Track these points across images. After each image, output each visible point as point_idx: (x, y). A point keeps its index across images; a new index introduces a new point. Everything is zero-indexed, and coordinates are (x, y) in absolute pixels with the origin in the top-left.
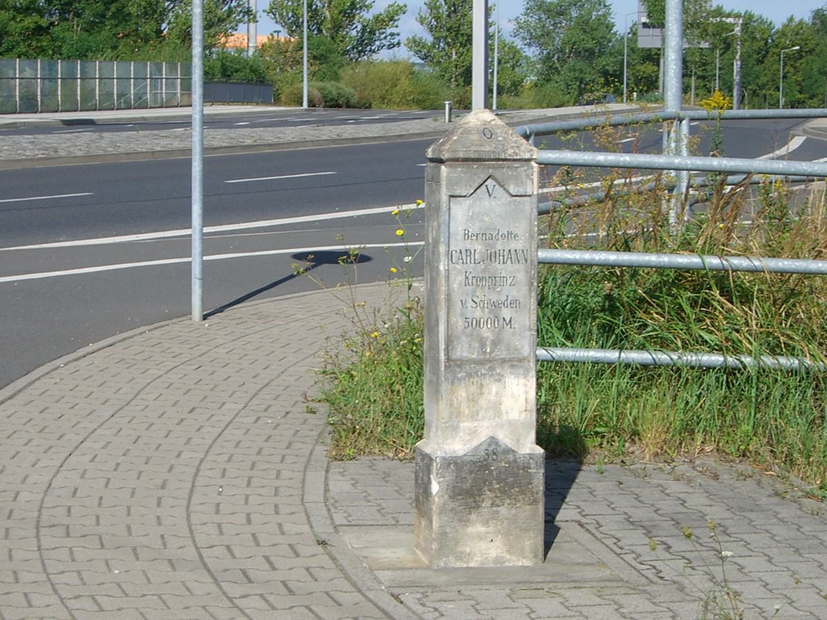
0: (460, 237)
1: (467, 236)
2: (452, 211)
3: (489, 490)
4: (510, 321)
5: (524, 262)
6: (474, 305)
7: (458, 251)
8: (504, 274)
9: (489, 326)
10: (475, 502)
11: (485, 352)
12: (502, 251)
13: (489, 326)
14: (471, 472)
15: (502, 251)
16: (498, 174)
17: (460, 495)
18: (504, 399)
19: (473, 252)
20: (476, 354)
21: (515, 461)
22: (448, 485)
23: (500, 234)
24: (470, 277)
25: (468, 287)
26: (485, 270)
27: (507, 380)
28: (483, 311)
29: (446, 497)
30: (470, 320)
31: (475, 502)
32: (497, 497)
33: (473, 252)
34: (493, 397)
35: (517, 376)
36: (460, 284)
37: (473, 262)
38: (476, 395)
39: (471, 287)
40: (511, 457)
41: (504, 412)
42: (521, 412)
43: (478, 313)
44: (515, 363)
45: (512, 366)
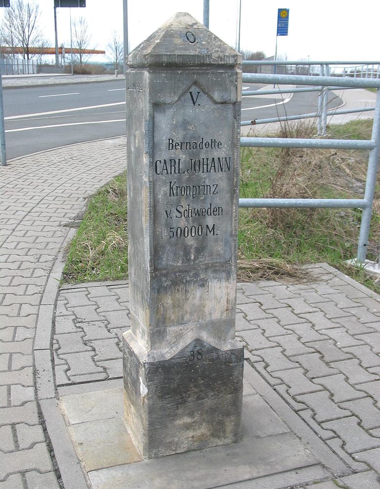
0: (164, 147)
1: (172, 145)
2: (156, 120)
3: (195, 387)
4: (213, 228)
5: (227, 170)
6: (179, 215)
7: (163, 161)
8: (207, 183)
9: (193, 235)
10: (182, 398)
11: (189, 260)
12: (205, 160)
13: (193, 235)
14: (178, 373)
15: (205, 160)
16: (203, 80)
17: (168, 394)
18: (207, 302)
19: (177, 161)
20: (181, 262)
21: (218, 358)
22: (156, 387)
23: (204, 143)
24: (174, 187)
25: (172, 197)
26: (189, 180)
27: (210, 283)
28: (187, 221)
29: (155, 398)
30: (174, 230)
31: (182, 398)
32: (201, 391)
33: (177, 161)
34: (197, 302)
35: (220, 280)
36: (165, 194)
37: (177, 171)
38: (181, 301)
39: (176, 197)
40: (214, 355)
41: (207, 313)
42: (222, 313)
43: (183, 223)
44: (218, 268)
45: (215, 271)
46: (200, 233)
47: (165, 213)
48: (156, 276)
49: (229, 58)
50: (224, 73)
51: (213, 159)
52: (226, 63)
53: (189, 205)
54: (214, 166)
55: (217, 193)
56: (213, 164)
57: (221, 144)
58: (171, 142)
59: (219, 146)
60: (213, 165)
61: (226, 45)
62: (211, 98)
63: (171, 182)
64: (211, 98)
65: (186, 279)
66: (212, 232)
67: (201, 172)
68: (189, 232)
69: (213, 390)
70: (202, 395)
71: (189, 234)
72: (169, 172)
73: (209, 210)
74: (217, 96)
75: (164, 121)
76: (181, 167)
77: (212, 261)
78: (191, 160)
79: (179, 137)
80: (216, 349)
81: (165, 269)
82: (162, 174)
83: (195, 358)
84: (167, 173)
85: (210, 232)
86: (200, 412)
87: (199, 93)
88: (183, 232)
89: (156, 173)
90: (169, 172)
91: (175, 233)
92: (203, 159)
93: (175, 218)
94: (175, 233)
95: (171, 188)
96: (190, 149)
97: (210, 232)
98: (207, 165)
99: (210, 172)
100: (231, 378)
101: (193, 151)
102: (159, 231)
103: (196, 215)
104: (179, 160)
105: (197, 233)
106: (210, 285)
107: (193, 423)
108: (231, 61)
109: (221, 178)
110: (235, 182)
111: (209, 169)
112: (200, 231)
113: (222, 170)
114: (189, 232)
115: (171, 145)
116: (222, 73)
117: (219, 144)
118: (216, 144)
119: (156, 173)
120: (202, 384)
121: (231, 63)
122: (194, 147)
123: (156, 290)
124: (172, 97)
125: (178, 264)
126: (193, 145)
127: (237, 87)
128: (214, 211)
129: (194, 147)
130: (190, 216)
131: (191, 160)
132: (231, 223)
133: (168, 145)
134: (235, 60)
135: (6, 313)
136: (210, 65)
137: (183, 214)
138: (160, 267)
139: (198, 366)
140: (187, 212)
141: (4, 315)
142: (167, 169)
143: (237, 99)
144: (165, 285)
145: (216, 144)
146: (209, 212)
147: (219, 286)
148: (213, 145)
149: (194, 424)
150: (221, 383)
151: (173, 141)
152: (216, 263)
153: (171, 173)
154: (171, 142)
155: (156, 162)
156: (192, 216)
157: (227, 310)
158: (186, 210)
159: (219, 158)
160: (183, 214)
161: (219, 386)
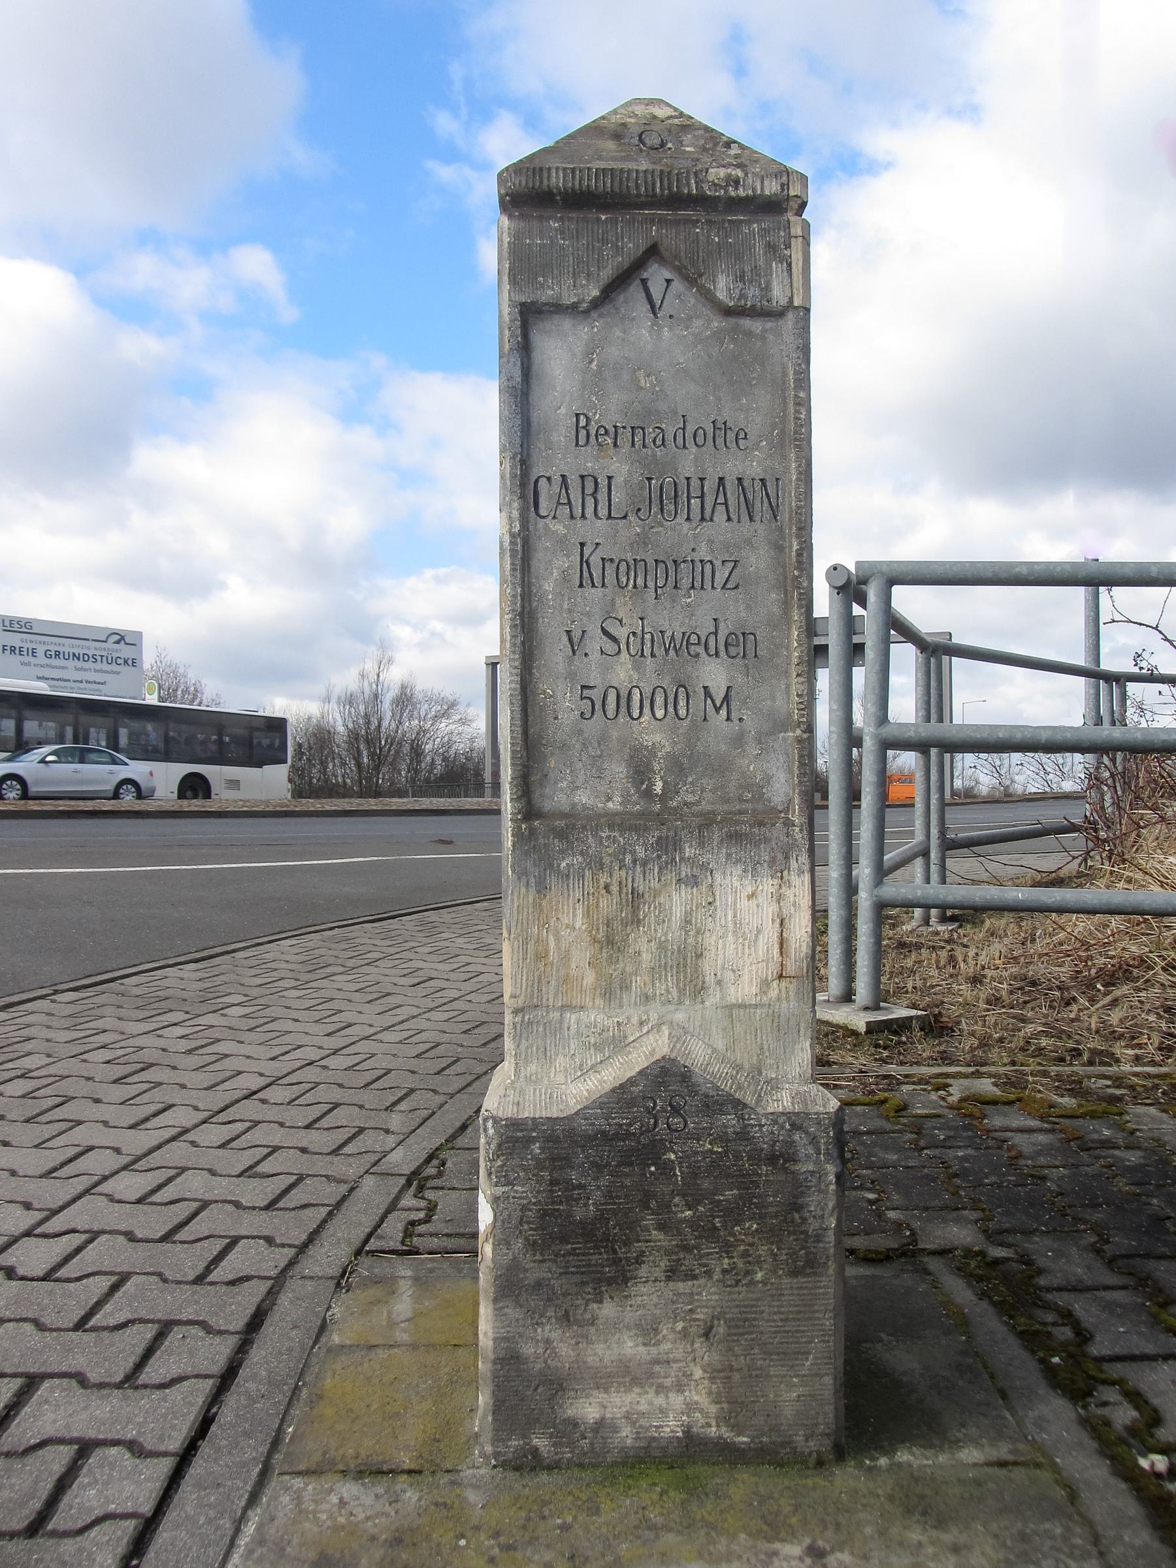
0: (561, 435)
1: (585, 432)
2: (536, 356)
3: (661, 1227)
4: (727, 698)
5: (768, 515)
6: (610, 647)
7: (557, 479)
8: (703, 553)
9: (660, 713)
10: (616, 1262)
11: (648, 794)
12: (695, 483)
13: (660, 713)
14: (599, 1167)
15: (695, 483)
16: (670, 239)
17: (564, 1240)
18: (710, 940)
19: (603, 483)
20: (617, 799)
21: (744, 1135)
22: (524, 1209)
23: (690, 429)
24: (595, 560)
25: (589, 591)
26: (643, 541)
27: (718, 876)
28: (637, 667)
29: (519, 1244)
30: (596, 695)
31: (616, 1262)
32: (686, 1248)
33: (603, 483)
34: (674, 934)
35: (752, 869)
36: (565, 578)
37: (603, 512)
38: (617, 925)
39: (598, 592)
40: (730, 1120)
41: (710, 979)
42: (765, 984)
43: (623, 673)
44: (745, 828)
45: (735, 837)
46: (682, 712)
47: (565, 638)
48: (532, 832)
49: (762, 182)
50: (749, 223)
51: (721, 479)
52: (750, 192)
53: (642, 619)
54: (726, 504)
55: (736, 587)
56: (721, 495)
57: (745, 438)
58: (583, 422)
59: (741, 442)
60: (721, 500)
61: (756, 152)
62: (708, 296)
63: (582, 545)
64: (708, 296)
65: (633, 853)
66: (723, 712)
67: (681, 519)
68: (647, 704)
69: (727, 1249)
70: (689, 1261)
71: (647, 710)
72: (578, 511)
73: (712, 638)
74: (723, 287)
75: (560, 352)
76: (615, 500)
77: (726, 807)
78: (649, 479)
79: (611, 410)
80: (739, 1105)
81: (563, 815)
82: (554, 517)
83: (662, 1125)
84: (572, 517)
85: (717, 710)
86: (680, 1326)
87: (668, 281)
88: (624, 701)
89: (537, 513)
90: (578, 511)
91: (598, 706)
92: (688, 479)
93: (597, 655)
94: (598, 706)
95: (584, 562)
96: (644, 446)
97: (717, 710)
98: (702, 497)
99: (711, 520)
100: (796, 1216)
101: (654, 456)
102: (544, 692)
103: (667, 651)
104: (610, 478)
105: (671, 709)
106: (717, 883)
107: (657, 1362)
108: (771, 188)
109: (748, 542)
110: (794, 554)
111: (707, 514)
112: (682, 703)
113: (751, 519)
114: (647, 704)
115: (583, 433)
116: (741, 221)
117: (741, 435)
118: (731, 436)
119: (537, 513)
120: (685, 1220)
121: (767, 192)
122: (659, 442)
123: (532, 880)
124: (582, 286)
125: (610, 805)
126: (653, 435)
127: (790, 265)
128: (727, 645)
129: (659, 442)
130: (647, 651)
131: (649, 479)
132: (788, 686)
133: (574, 432)
134: (782, 185)
135: (266, 1233)
136: (701, 201)
137: (623, 646)
138: (547, 806)
139: (673, 1156)
140: (639, 640)
141: (260, 1237)
142: (569, 503)
143: (791, 299)
144: (563, 864)
145: (731, 436)
146: (712, 643)
147: (749, 890)
148: (720, 441)
149: (657, 1368)
150: (757, 1230)
151: (588, 420)
152: (740, 812)
153: (583, 516)
154: (583, 422)
155: (537, 482)
156: (653, 655)
157: (781, 976)
158: (634, 634)
159: (740, 480)
160: (623, 646)
161: (750, 1239)
